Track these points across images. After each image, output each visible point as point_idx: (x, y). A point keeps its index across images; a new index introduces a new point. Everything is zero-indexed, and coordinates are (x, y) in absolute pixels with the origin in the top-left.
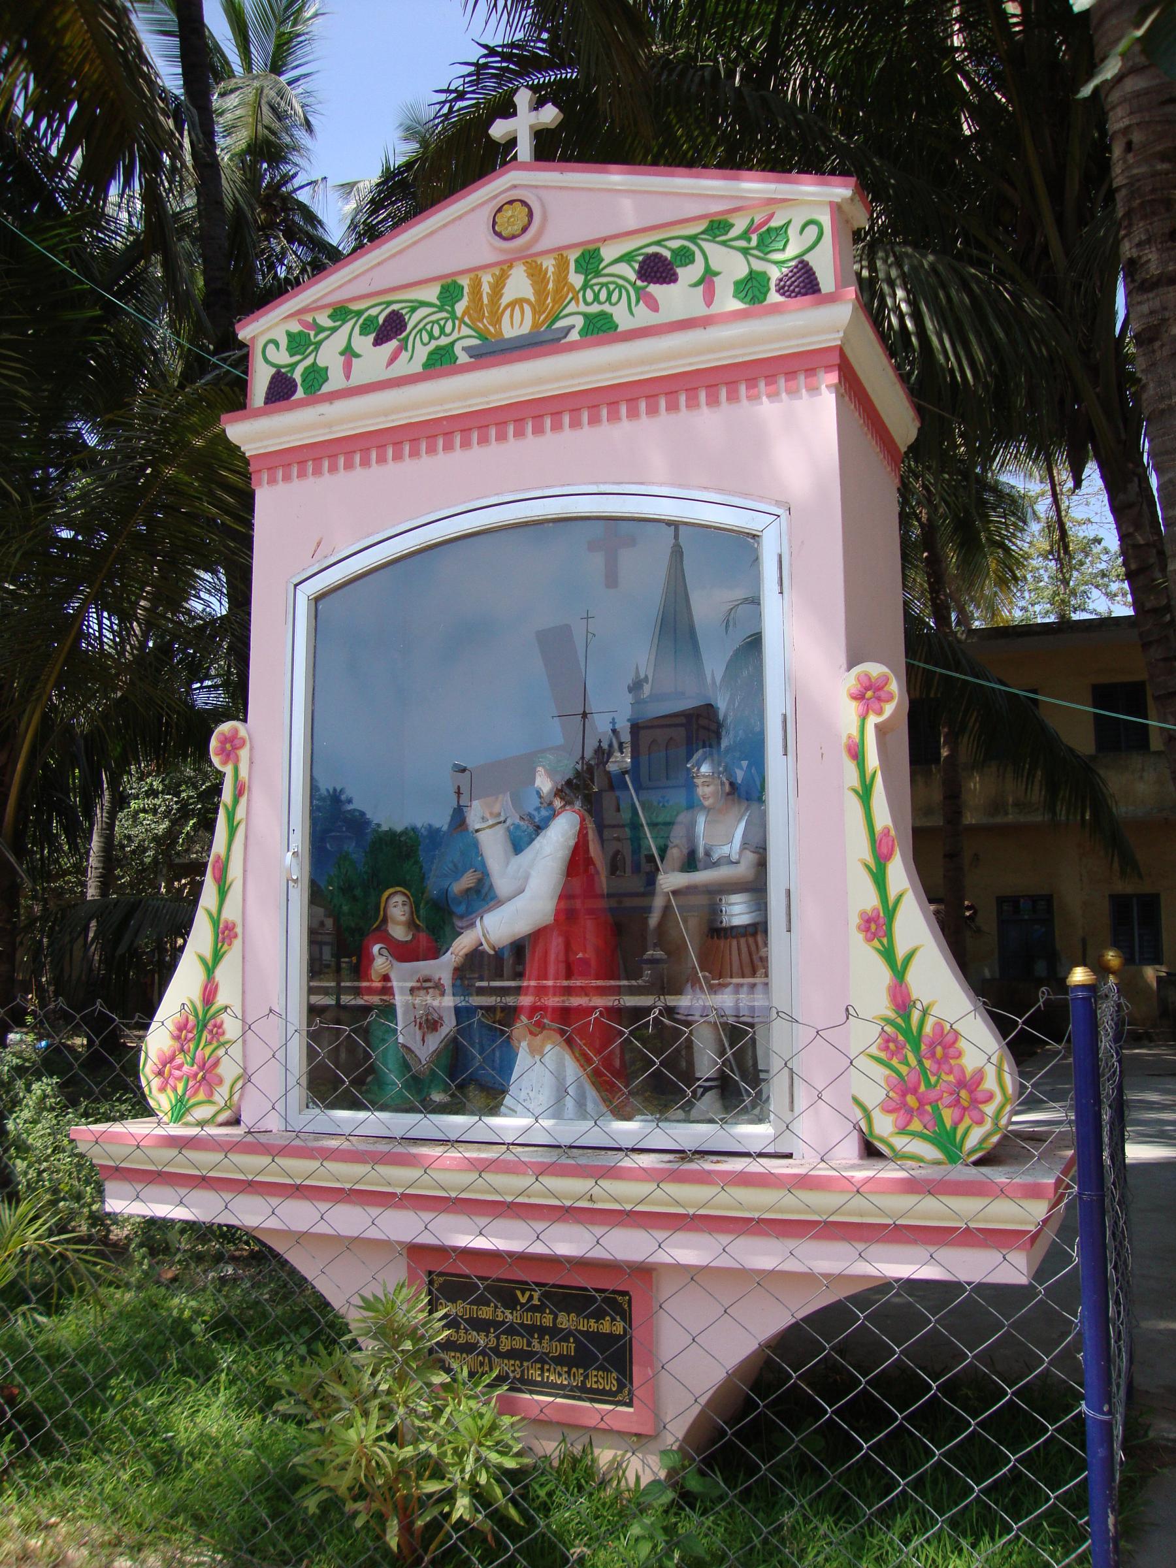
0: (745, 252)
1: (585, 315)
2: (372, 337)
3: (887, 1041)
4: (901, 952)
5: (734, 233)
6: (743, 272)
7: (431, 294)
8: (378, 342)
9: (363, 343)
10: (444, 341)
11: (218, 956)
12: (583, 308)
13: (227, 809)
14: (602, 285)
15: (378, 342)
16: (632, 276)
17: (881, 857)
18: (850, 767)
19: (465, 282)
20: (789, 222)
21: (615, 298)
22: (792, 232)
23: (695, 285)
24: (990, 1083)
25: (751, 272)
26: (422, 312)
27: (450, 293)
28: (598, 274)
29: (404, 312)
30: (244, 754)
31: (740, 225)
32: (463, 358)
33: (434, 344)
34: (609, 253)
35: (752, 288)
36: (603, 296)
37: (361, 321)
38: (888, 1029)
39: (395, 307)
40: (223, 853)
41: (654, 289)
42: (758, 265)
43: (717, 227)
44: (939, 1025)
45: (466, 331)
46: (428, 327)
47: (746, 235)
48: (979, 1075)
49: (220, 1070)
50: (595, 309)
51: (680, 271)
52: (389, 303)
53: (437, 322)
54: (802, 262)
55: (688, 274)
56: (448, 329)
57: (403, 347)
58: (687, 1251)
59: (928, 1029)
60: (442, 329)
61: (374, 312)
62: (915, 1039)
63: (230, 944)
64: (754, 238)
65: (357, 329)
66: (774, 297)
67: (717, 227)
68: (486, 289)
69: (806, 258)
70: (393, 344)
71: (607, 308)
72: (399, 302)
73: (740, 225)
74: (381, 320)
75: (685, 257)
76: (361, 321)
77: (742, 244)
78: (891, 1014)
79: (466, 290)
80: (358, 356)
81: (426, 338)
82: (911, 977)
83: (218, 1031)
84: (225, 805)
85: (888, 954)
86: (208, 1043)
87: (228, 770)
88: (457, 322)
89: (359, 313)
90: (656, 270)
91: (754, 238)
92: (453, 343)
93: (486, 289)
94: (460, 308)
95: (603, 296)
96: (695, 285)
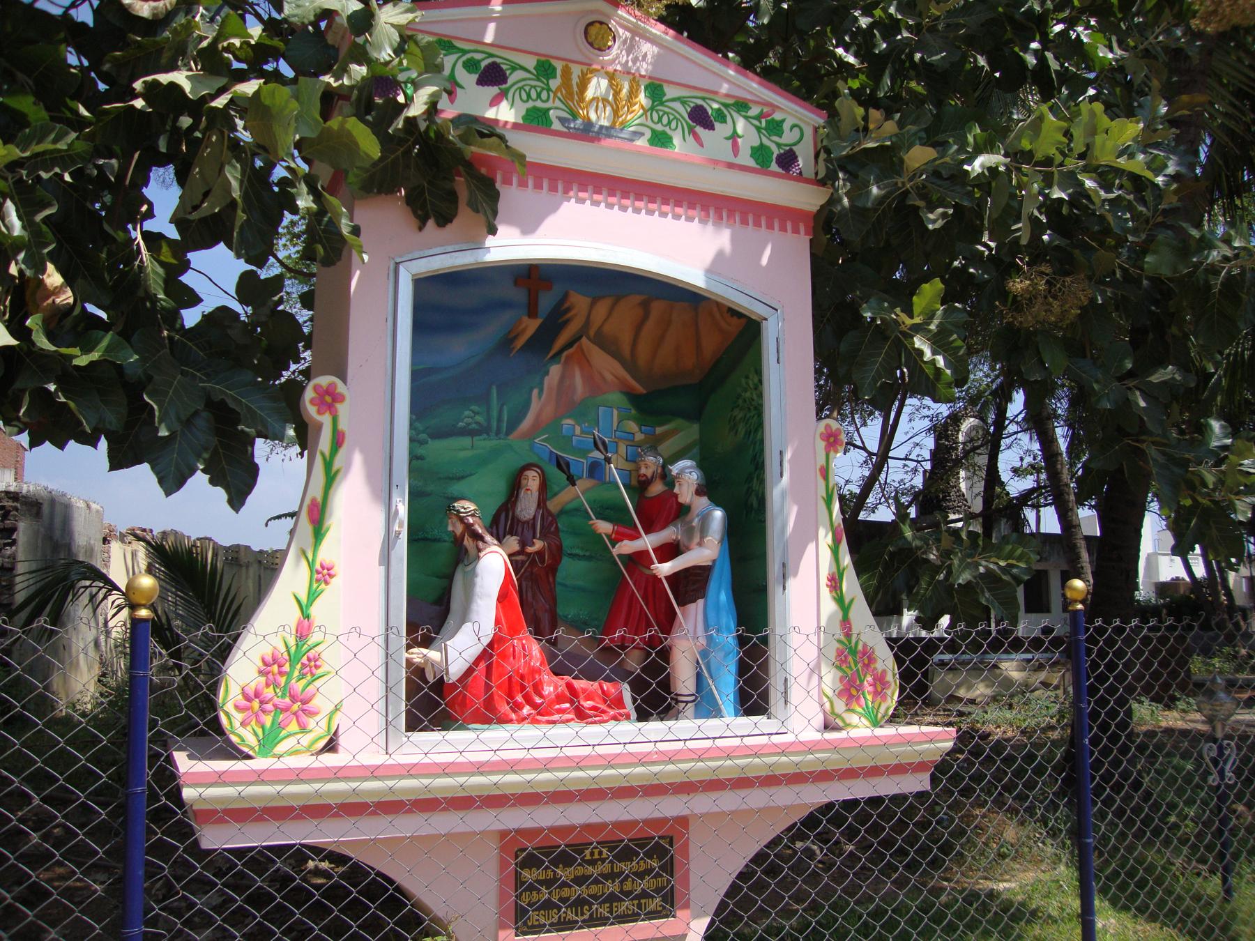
0: (758, 129)
1: (653, 131)
2: (475, 77)
3: (840, 653)
4: (847, 601)
5: (750, 113)
6: (756, 143)
7: (530, 62)
8: (481, 82)
9: (468, 79)
10: (539, 104)
11: (313, 596)
12: (650, 123)
13: (324, 458)
14: (665, 113)
15: (481, 82)
16: (686, 116)
17: (836, 541)
18: (821, 482)
19: (559, 65)
20: (783, 121)
21: (673, 125)
22: (786, 126)
23: (727, 139)
24: (889, 678)
25: (762, 144)
26: (519, 75)
27: (545, 70)
28: (662, 104)
29: (504, 67)
30: (342, 408)
31: (755, 111)
32: (557, 126)
33: (530, 104)
34: (670, 92)
35: (760, 153)
36: (665, 120)
37: (464, 58)
38: (840, 647)
39: (498, 60)
40: (319, 499)
41: (699, 129)
42: (766, 142)
43: (741, 106)
44: (865, 645)
45: (558, 104)
46: (527, 88)
47: (759, 117)
48: (884, 672)
49: (316, 703)
50: (659, 127)
51: (717, 125)
52: (491, 55)
53: (535, 87)
54: (791, 150)
55: (722, 130)
56: (544, 95)
57: (502, 95)
58: (700, 804)
59: (860, 647)
60: (539, 96)
61: (478, 56)
62: (853, 651)
63: (327, 583)
64: (763, 121)
65: (460, 63)
66: (774, 167)
67: (741, 106)
68: (575, 80)
69: (794, 148)
70: (495, 90)
71: (667, 129)
72: (505, 57)
73: (755, 111)
74: (483, 65)
75: (722, 117)
76: (464, 58)
77: (756, 123)
78: (842, 638)
79: (559, 72)
80: (462, 87)
81: (524, 97)
82: (852, 615)
83: (311, 665)
84: (323, 454)
85: (839, 600)
86: (303, 676)
87: (326, 419)
88: (552, 95)
89: (465, 52)
90: (700, 117)
91: (763, 121)
92: (549, 109)
93: (575, 80)
94: (554, 84)
95: (665, 120)
96: (727, 139)
